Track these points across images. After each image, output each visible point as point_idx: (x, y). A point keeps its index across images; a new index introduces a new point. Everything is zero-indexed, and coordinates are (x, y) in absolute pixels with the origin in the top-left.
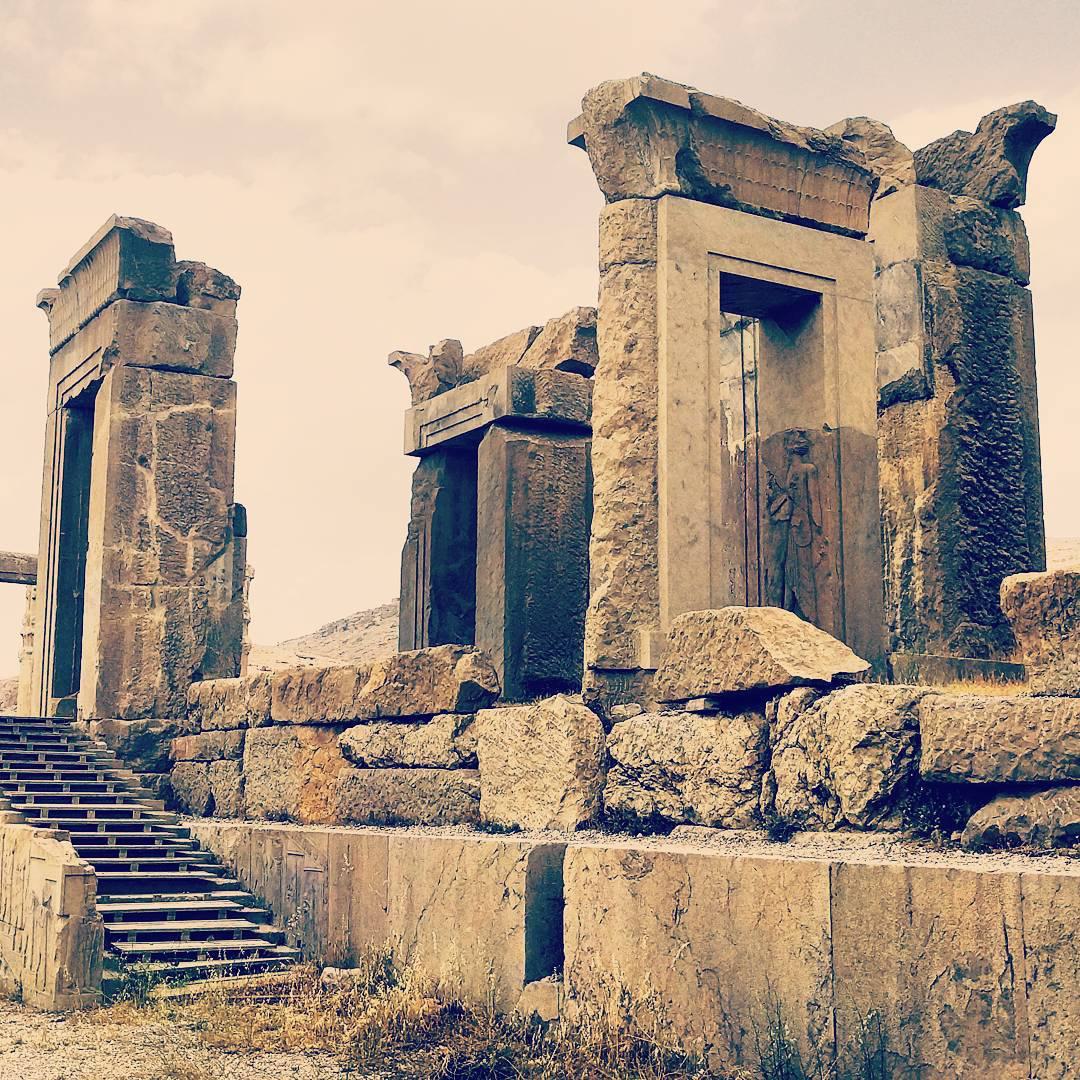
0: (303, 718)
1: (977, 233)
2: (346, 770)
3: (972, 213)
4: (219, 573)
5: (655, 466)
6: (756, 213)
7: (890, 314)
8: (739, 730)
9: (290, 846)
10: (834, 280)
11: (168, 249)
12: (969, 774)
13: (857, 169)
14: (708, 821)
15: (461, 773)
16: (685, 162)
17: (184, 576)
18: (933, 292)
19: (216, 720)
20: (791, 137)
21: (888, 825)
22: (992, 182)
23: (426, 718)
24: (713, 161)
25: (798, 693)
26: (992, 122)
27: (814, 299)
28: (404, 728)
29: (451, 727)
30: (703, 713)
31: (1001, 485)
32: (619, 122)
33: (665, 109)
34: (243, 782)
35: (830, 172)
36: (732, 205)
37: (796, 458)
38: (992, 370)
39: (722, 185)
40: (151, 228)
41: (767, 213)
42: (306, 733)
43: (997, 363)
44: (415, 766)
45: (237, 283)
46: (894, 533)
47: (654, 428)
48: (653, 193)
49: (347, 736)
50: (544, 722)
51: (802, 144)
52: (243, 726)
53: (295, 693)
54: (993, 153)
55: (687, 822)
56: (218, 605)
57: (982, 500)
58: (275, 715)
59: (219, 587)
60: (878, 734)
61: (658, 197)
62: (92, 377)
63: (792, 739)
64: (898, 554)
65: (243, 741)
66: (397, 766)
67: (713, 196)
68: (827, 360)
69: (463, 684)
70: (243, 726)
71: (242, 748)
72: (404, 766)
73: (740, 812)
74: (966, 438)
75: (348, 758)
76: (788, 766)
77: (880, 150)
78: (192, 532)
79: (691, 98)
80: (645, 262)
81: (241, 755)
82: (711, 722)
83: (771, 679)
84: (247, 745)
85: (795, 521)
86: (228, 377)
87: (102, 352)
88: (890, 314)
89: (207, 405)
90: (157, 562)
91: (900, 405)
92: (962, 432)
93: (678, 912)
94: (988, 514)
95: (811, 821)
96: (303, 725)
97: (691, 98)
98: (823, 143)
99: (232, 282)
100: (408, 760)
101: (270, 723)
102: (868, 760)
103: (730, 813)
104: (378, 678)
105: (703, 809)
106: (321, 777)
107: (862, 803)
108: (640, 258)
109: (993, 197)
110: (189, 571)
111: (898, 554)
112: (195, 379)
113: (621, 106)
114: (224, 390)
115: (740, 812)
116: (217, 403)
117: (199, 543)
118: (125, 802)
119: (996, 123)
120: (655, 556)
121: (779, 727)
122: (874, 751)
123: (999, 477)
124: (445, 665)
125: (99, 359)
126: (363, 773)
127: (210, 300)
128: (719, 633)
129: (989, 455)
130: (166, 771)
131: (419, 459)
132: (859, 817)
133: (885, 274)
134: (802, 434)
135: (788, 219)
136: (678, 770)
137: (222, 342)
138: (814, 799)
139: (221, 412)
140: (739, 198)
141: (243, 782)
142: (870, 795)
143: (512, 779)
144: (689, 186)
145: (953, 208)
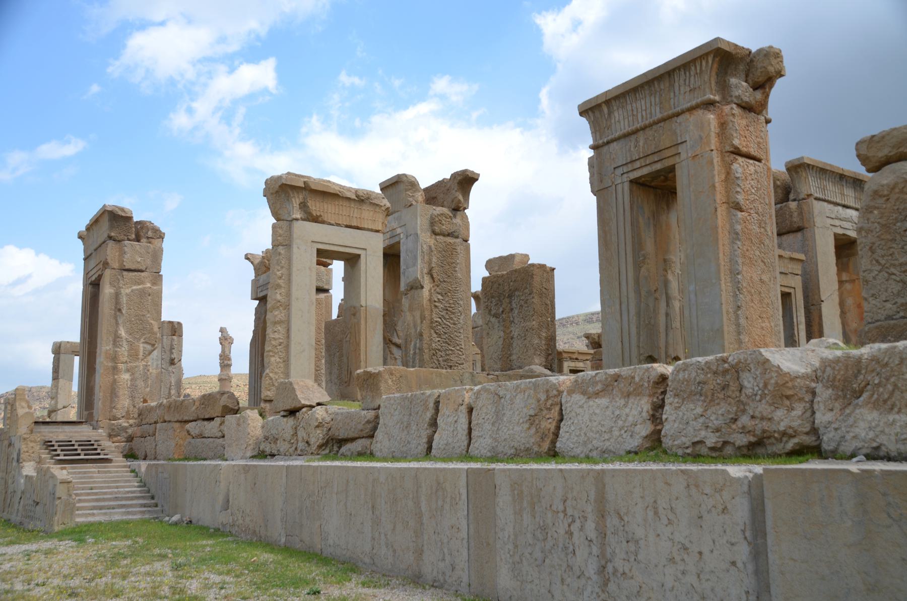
0: (176, 420)
1: (444, 222)
2: (189, 439)
3: (442, 214)
4: (155, 357)
5: (288, 323)
6: (333, 225)
7: (410, 254)
8: (291, 421)
9: (160, 470)
10: (366, 249)
11: (130, 218)
12: (339, 436)
13: (377, 205)
14: (283, 454)
15: (221, 439)
16: (303, 206)
17: (138, 359)
18: (425, 246)
19: (147, 420)
20: (349, 195)
21: (324, 452)
22: (453, 201)
23: (213, 419)
24: (315, 206)
25: (304, 410)
26: (454, 176)
27: (359, 256)
28: (206, 423)
29: (219, 423)
30: (284, 416)
31: (452, 322)
32: (277, 192)
33: (294, 188)
34: (156, 445)
35: (365, 207)
36: (323, 222)
37: (352, 316)
38: (449, 276)
39: (318, 214)
40: (122, 210)
41: (338, 225)
42: (178, 425)
43: (452, 273)
44: (209, 438)
45: (163, 231)
46: (411, 341)
47: (289, 309)
48: (290, 219)
49: (189, 426)
50: (242, 421)
51: (354, 197)
52: (156, 423)
53: (173, 409)
54: (454, 189)
55: (278, 455)
56: (154, 371)
57: (443, 328)
58: (167, 418)
59: (155, 364)
60: (321, 423)
61: (291, 221)
62: (100, 273)
63: (301, 426)
64: (412, 349)
65: (156, 429)
66: (203, 437)
67: (316, 220)
68: (363, 280)
69: (223, 406)
70: (156, 423)
71: (155, 431)
72: (205, 437)
73: (290, 450)
74: (437, 304)
75: (189, 434)
76: (301, 434)
77: (410, 187)
78: (142, 340)
79: (305, 182)
80: (286, 245)
81: (155, 435)
82: (285, 419)
83: (298, 406)
84: (157, 430)
85: (351, 341)
86: (159, 273)
87: (102, 263)
88: (410, 254)
89: (149, 285)
90: (126, 354)
91: (413, 290)
92: (435, 301)
93: (255, 484)
94: (445, 333)
95: (306, 452)
96: (176, 422)
97: (305, 182)
98: (362, 196)
99: (160, 231)
100: (206, 436)
101: (165, 422)
102: (318, 432)
103: (288, 450)
104: (197, 404)
105: (281, 450)
106: (182, 442)
107: (316, 446)
108: (284, 244)
109: (453, 207)
110: (141, 356)
111: (412, 349)
112: (143, 274)
113: (277, 186)
114: (157, 278)
115: (291, 450)
116: (154, 284)
117: (145, 345)
118: (104, 455)
119: (455, 177)
120: (288, 358)
121: (300, 420)
122: (320, 428)
123: (451, 318)
124: (217, 399)
125: (101, 266)
126: (193, 441)
127: (151, 240)
128: (287, 389)
129: (447, 310)
130: (131, 441)
131: (257, 302)
132: (315, 450)
133: (409, 238)
134: (354, 308)
135: (347, 226)
136: (277, 437)
137: (157, 257)
138: (306, 445)
139: (155, 288)
140: (326, 219)
141: (156, 445)
142: (318, 443)
143: (233, 441)
144: (306, 215)
145: (434, 212)
